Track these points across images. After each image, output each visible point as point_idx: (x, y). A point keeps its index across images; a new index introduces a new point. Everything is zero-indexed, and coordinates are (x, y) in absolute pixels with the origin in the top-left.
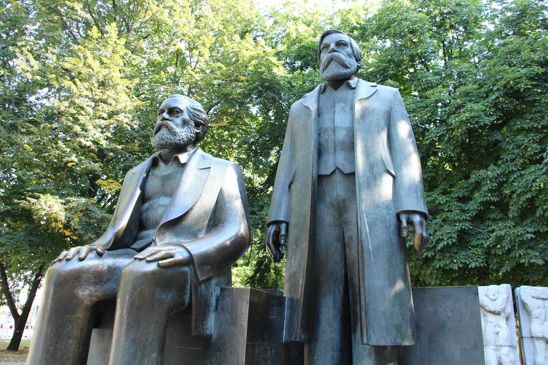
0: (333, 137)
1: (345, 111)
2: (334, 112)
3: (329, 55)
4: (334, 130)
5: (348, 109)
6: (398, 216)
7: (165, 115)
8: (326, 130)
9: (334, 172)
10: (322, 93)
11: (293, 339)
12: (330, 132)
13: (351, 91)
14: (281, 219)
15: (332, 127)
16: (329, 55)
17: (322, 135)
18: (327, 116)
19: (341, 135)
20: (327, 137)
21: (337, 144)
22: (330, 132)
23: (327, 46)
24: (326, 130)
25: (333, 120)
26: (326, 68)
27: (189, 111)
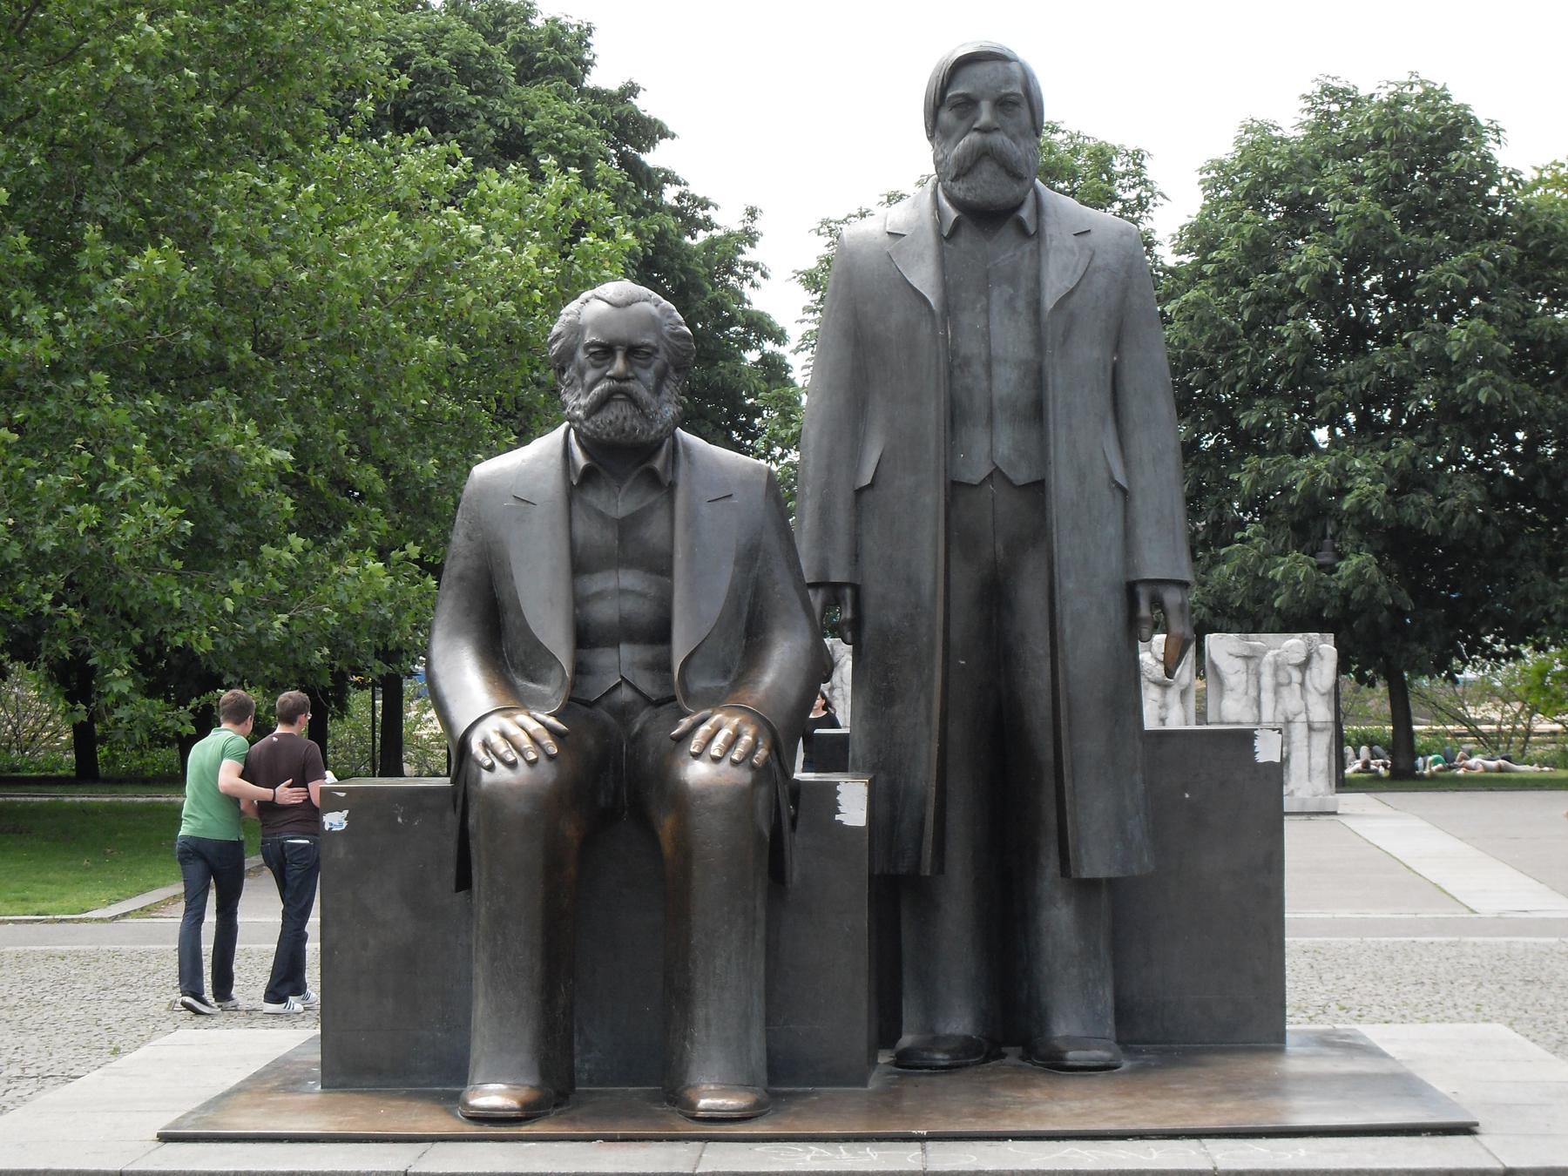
0: (985, 384)
1: (1013, 310)
2: (987, 311)
3: (974, 137)
4: (988, 366)
5: (1021, 304)
6: (1131, 590)
7: (619, 365)
8: (967, 362)
9: (991, 474)
10: (948, 239)
11: (904, 868)
12: (978, 369)
13: (1028, 246)
14: (837, 576)
15: (983, 358)
16: (974, 137)
17: (957, 373)
18: (969, 319)
19: (1007, 382)
20: (969, 380)
21: (996, 403)
22: (978, 369)
23: (968, 104)
24: (967, 362)
25: (986, 335)
26: (964, 175)
27: (669, 343)
